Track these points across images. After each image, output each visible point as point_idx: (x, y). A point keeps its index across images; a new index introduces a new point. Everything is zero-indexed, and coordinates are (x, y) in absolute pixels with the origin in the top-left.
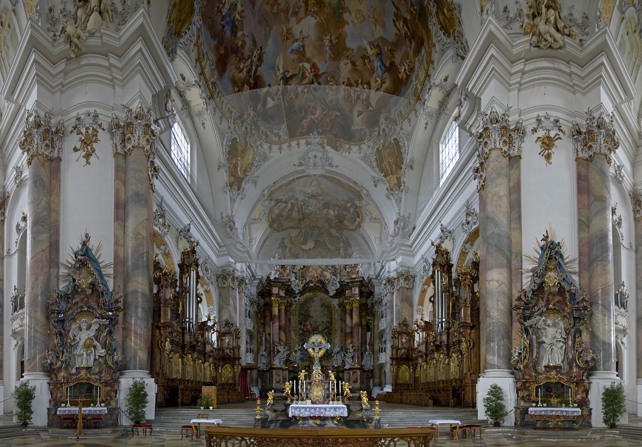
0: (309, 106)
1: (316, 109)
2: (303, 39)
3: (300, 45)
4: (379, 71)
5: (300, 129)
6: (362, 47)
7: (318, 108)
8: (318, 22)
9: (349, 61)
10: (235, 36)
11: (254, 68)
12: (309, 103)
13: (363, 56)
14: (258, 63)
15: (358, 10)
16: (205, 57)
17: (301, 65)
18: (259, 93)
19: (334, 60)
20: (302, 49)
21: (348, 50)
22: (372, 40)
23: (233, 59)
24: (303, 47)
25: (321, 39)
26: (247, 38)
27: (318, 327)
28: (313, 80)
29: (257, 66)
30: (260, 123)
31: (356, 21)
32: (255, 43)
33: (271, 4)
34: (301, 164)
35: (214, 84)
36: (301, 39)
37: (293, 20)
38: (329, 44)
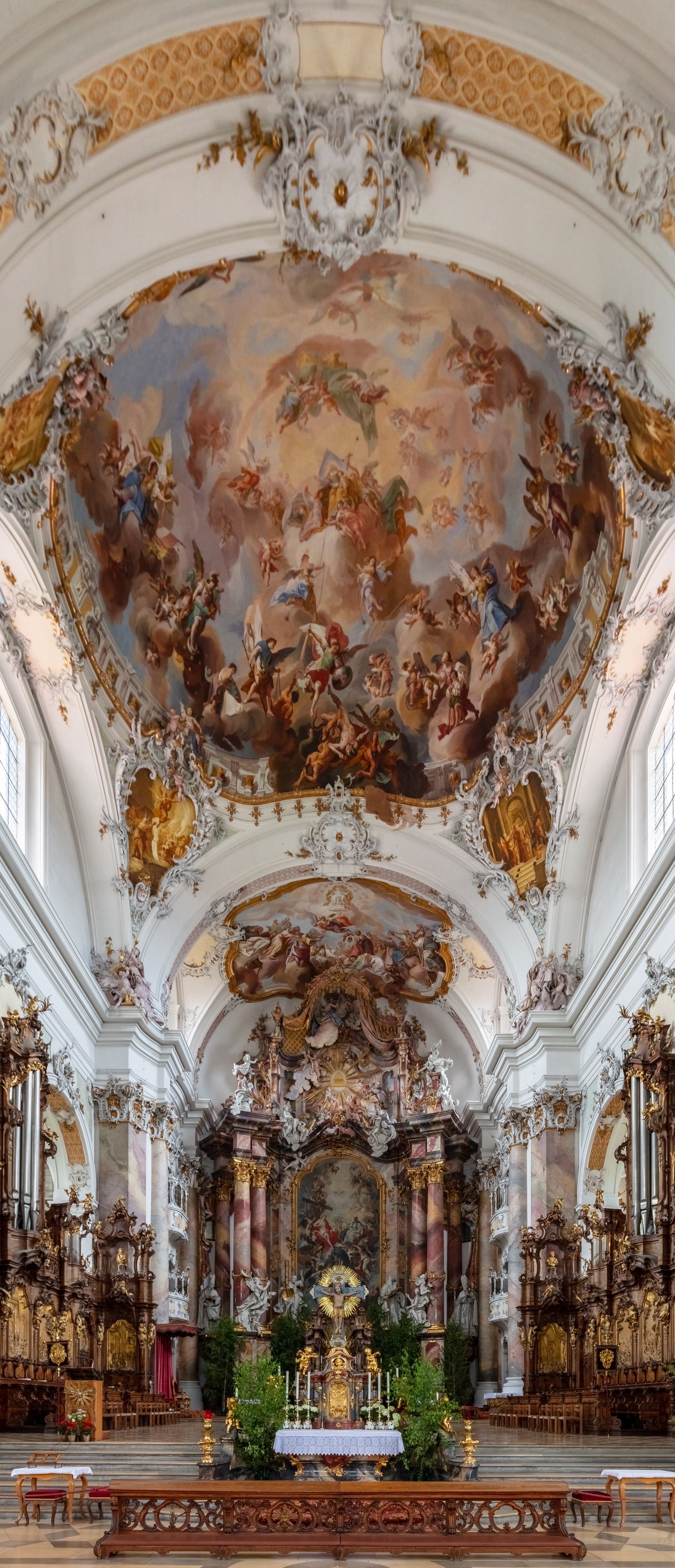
0: (325, 722)
1: (341, 729)
2: (310, 571)
3: (302, 585)
4: (492, 625)
5: (303, 773)
6: (449, 578)
7: (345, 727)
8: (344, 537)
9: (417, 616)
10: (152, 534)
11: (197, 618)
12: (325, 715)
13: (452, 599)
14: (206, 609)
15: (438, 500)
16: (71, 553)
17: (305, 628)
18: (209, 679)
19: (382, 616)
20: (306, 594)
21: (414, 590)
22: (473, 557)
23: (144, 583)
24: (310, 589)
25: (352, 572)
26: (181, 547)
27: (344, 1233)
28: (333, 662)
29: (205, 618)
30: (209, 748)
31: (434, 525)
32: (199, 562)
33: (241, 490)
34: (305, 854)
35: (93, 624)
36: (306, 573)
37: (293, 532)
38: (371, 583)
